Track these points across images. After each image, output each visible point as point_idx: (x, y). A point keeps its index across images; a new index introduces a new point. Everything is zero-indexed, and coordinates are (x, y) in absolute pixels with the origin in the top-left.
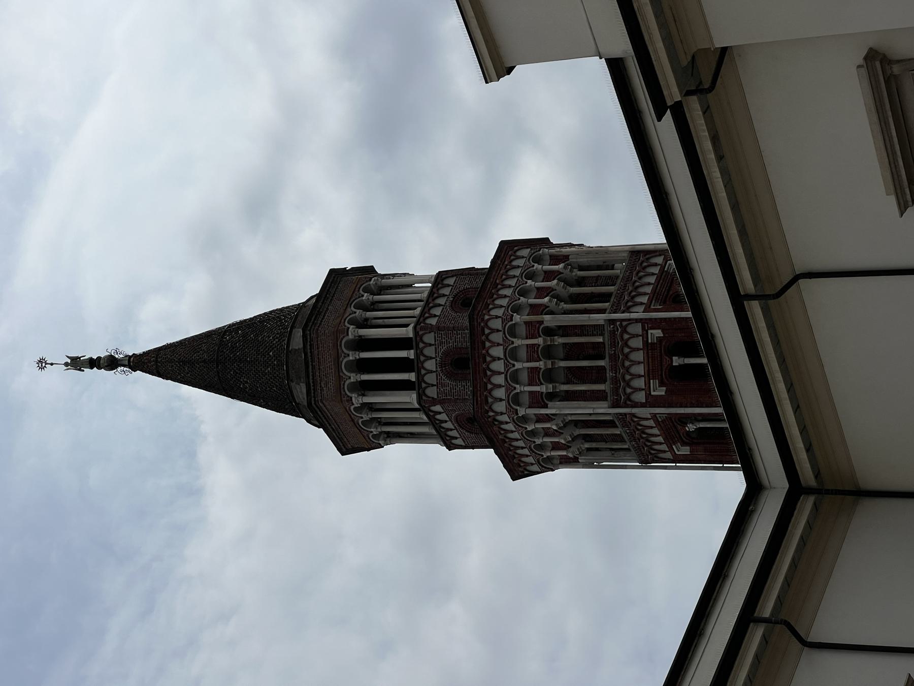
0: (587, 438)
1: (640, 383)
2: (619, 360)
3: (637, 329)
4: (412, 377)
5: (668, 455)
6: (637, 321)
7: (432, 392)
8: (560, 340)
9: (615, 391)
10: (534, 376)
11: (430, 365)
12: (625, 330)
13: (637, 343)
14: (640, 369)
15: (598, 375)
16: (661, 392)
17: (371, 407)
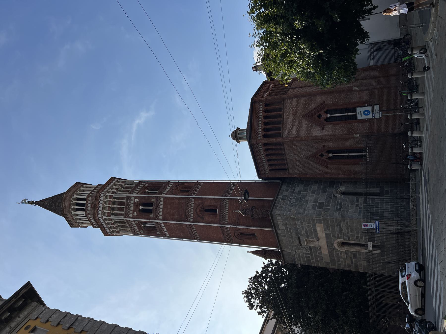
0: (122, 226)
1: (131, 212)
2: (128, 205)
3: (133, 198)
4: (84, 208)
5: (139, 233)
6: (133, 196)
7: (88, 212)
8: (116, 200)
9: (125, 214)
10: (109, 208)
11: (89, 205)
13: (132, 202)
14: (132, 208)
15: (121, 209)
16: (135, 214)
17: (77, 215)
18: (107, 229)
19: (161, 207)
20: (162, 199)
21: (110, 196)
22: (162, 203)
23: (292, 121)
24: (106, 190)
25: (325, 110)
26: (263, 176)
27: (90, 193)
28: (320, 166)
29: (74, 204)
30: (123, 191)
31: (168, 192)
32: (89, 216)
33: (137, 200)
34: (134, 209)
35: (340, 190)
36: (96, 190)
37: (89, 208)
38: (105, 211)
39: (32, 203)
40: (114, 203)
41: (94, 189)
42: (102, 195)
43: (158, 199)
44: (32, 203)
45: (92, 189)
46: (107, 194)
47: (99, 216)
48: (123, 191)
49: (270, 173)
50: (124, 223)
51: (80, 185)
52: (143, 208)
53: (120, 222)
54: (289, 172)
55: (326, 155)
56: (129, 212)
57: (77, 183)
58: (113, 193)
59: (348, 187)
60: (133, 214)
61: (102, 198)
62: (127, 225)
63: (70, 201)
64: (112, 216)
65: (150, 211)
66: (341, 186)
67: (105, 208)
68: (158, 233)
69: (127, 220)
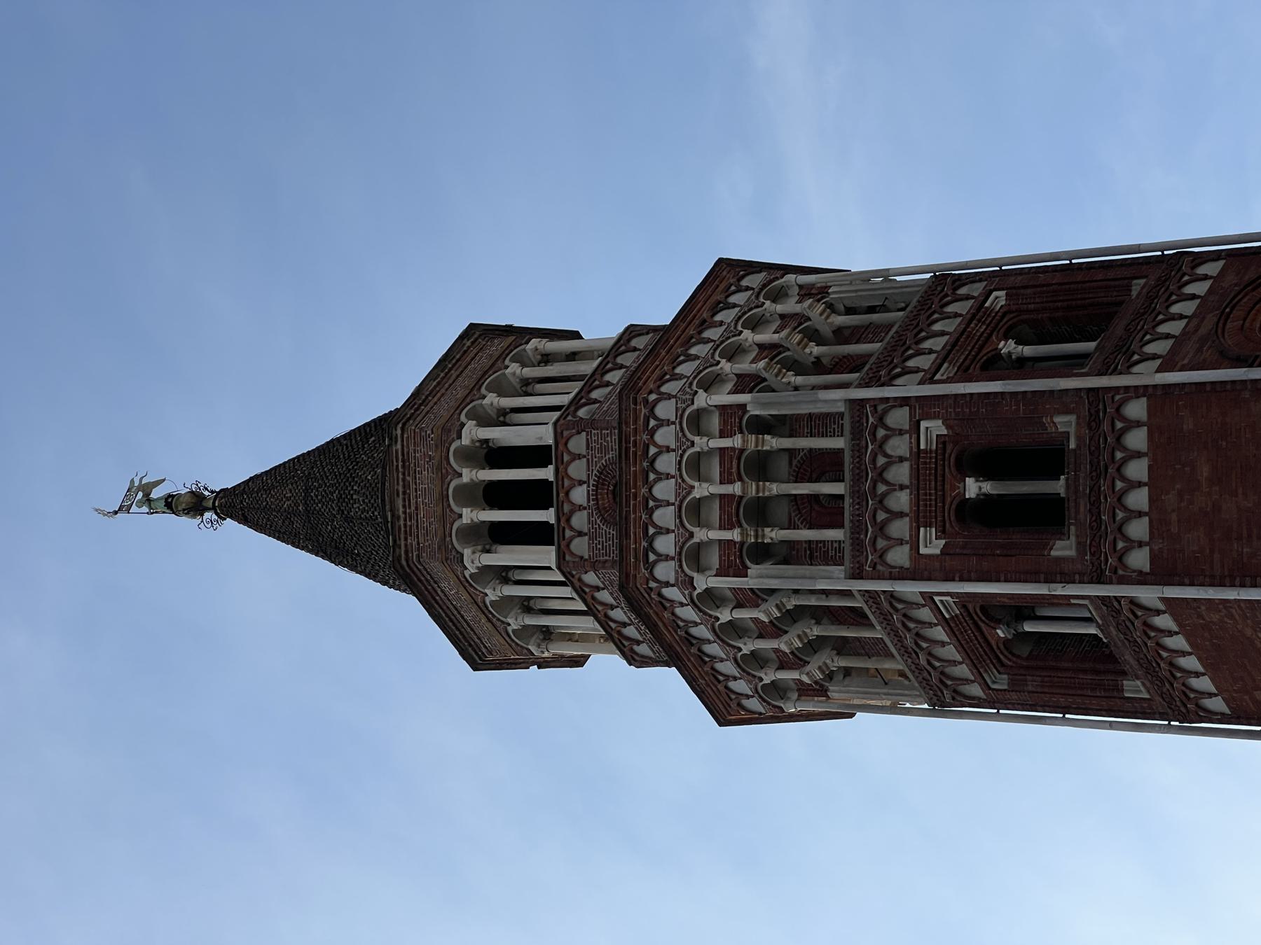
0: (842, 647)
1: (900, 528)
2: (868, 479)
3: (898, 418)
4: (548, 516)
5: (976, 690)
6: (904, 401)
7: (580, 546)
8: (772, 442)
9: (857, 545)
10: (732, 512)
11: (579, 495)
12: (881, 420)
13: (899, 446)
14: (902, 501)
16: (932, 545)
17: (503, 574)
18: (727, 668)
19: (1138, 470)
20: (1136, 409)
21: (723, 408)
22: (1137, 439)
24: (686, 369)
27: (576, 403)
29: (471, 495)
30: (818, 367)
31: (1179, 341)
32: (591, 578)
33: (933, 428)
34: (916, 501)
36: (614, 377)
37: (579, 521)
38: (701, 535)
39: (194, 504)
40: (760, 466)
41: (602, 370)
42: (665, 410)
43: (1098, 407)
44: (194, 504)
45: (587, 367)
46: (702, 400)
47: (665, 571)
48: (818, 367)
50: (856, 617)
51: (498, 345)
52: (988, 487)
53: (819, 615)
56: (881, 528)
57: (476, 334)
58: (746, 383)
60: (915, 547)
61: (665, 436)
62: (878, 633)
63: (444, 473)
64: (754, 569)
65: (1048, 516)
67: (695, 511)
68: (1134, 688)
69: (871, 596)
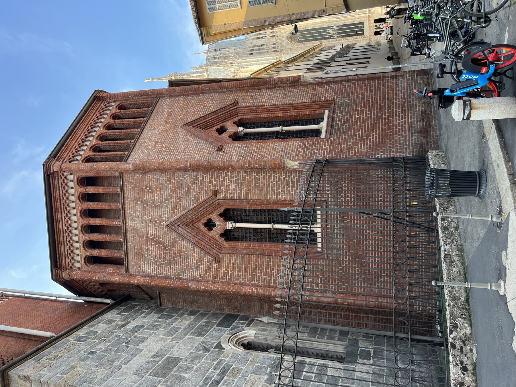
23: (160, 133)
25: (236, 119)
26: (65, 275)
28: (203, 255)
35: (241, 334)
49: (85, 268)
54: (127, 270)
55: (221, 225)
59: (265, 330)
66: (247, 326)
